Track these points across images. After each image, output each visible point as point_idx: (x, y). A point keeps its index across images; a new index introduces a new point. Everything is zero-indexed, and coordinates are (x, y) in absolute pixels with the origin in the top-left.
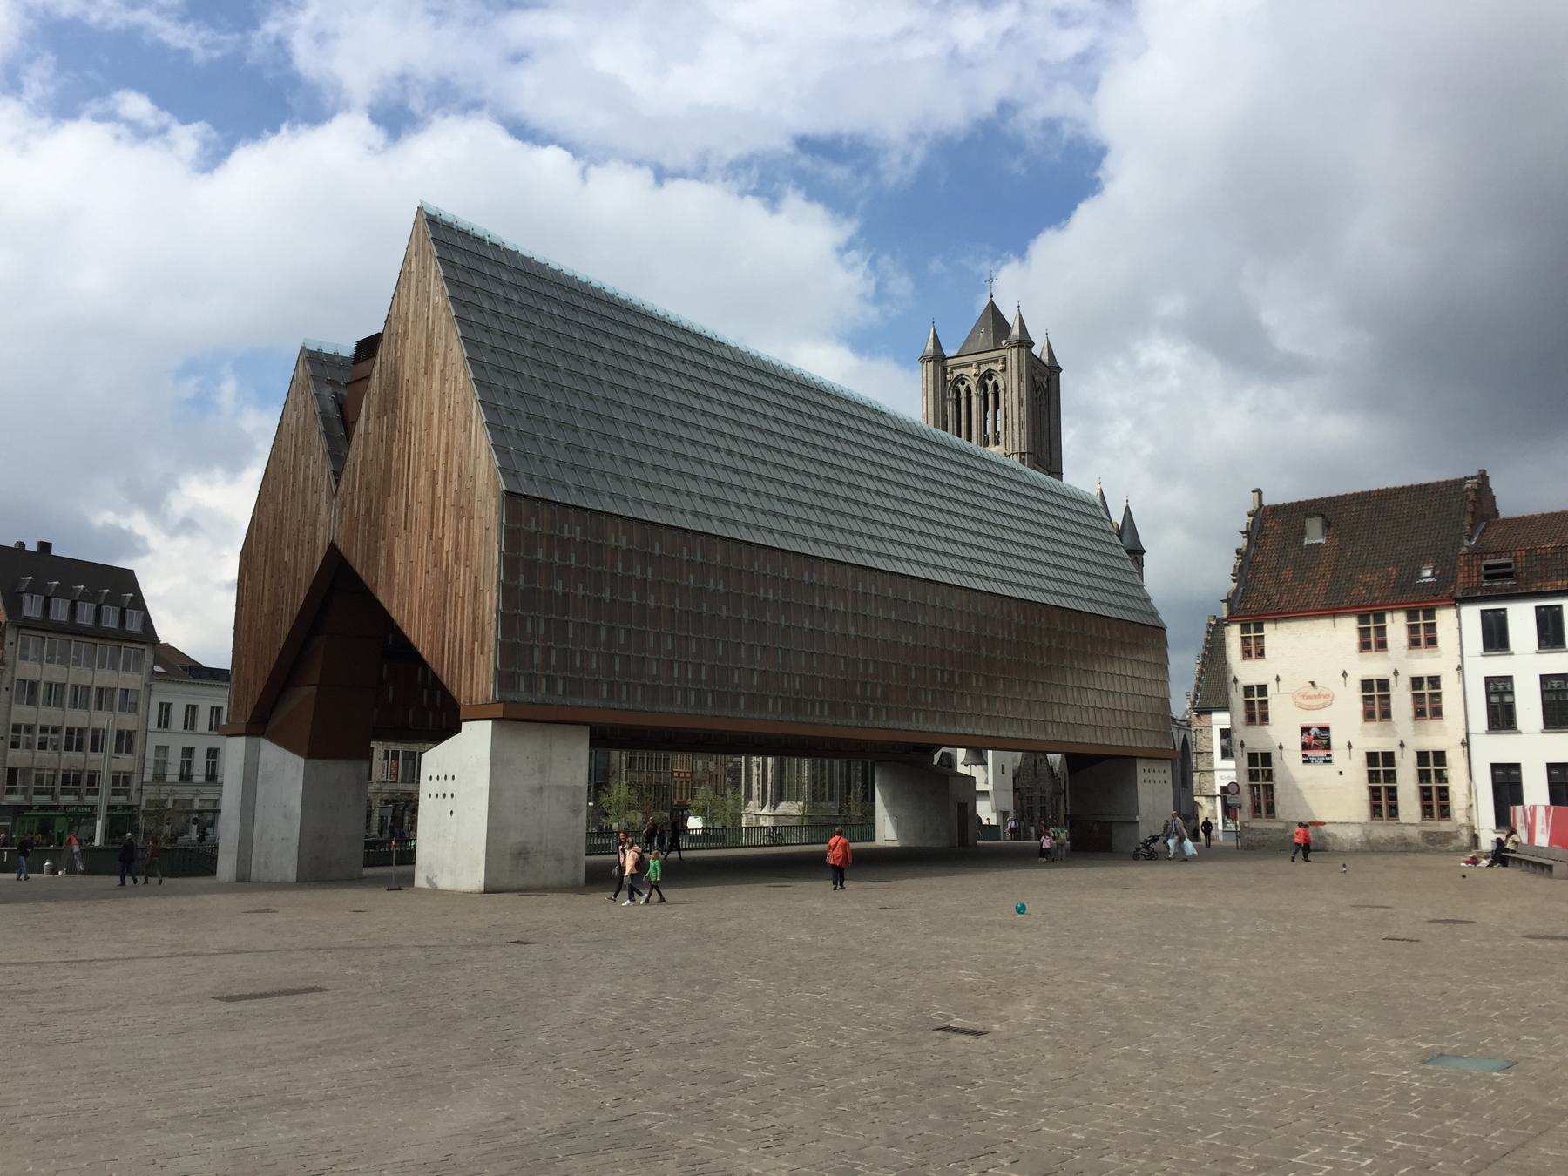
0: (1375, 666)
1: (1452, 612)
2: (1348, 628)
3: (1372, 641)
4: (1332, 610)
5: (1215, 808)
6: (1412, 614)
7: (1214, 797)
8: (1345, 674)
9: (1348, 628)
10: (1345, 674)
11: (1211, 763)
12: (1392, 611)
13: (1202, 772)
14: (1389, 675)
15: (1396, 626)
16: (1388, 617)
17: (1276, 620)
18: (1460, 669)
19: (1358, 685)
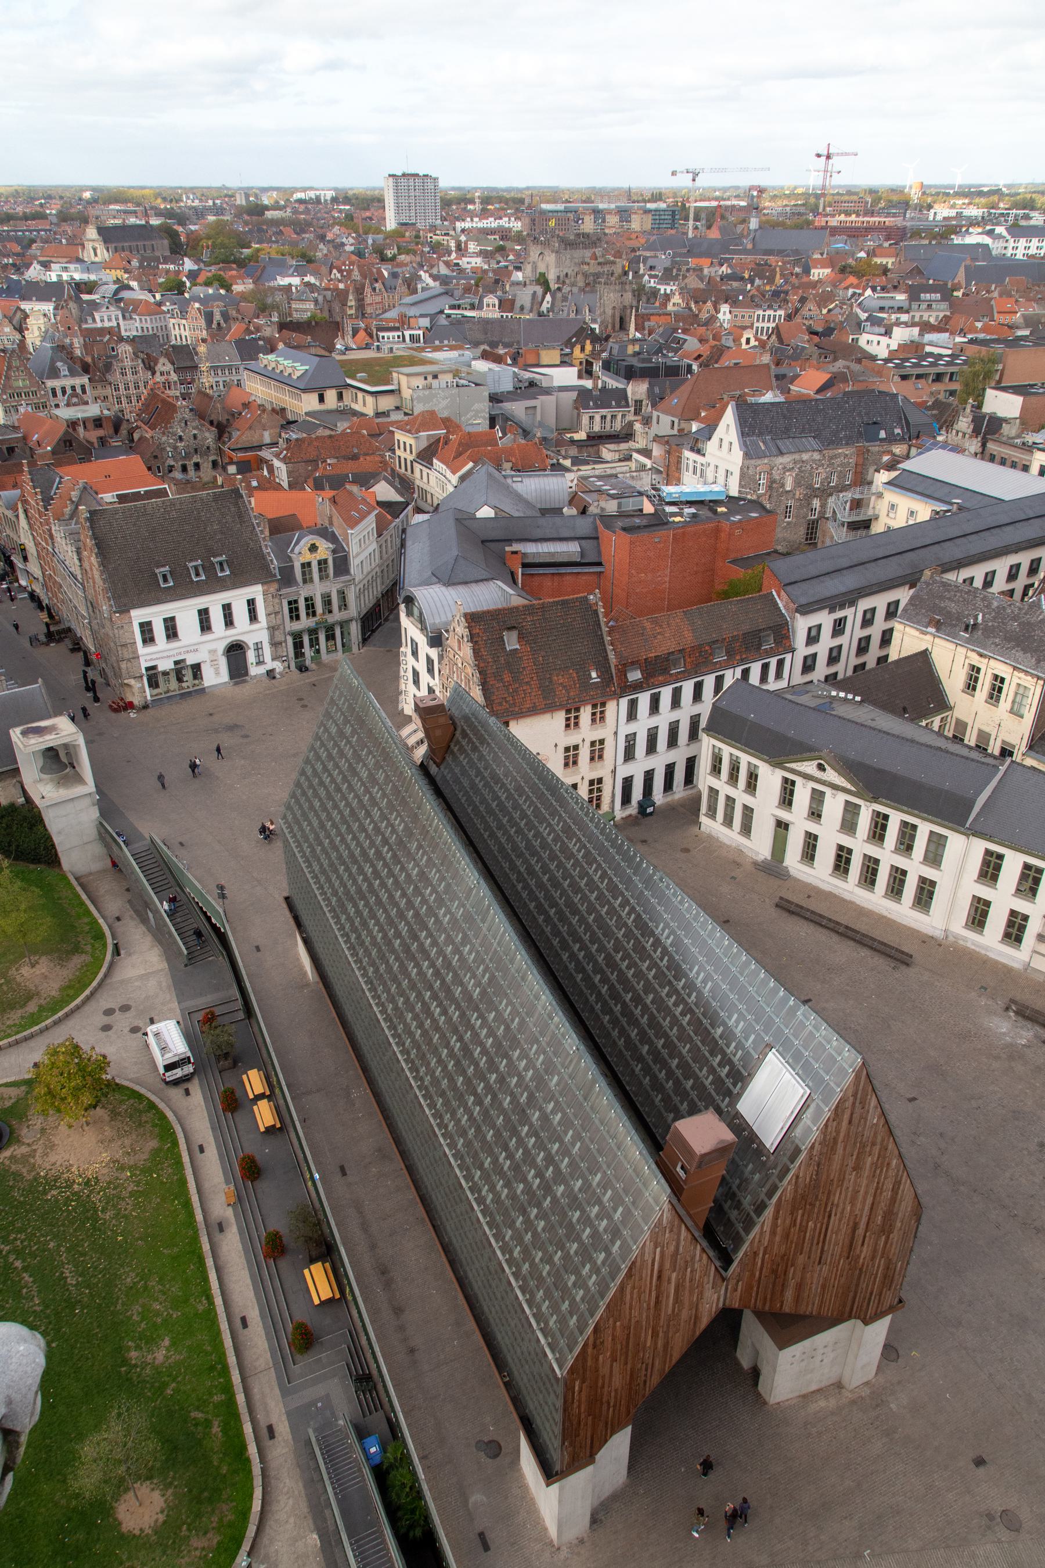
0: (573, 739)
1: (615, 702)
2: (560, 717)
3: (572, 724)
4: (550, 708)
5: (143, 684)
6: (594, 706)
7: (141, 677)
8: (556, 745)
9: (560, 717)
10: (556, 745)
11: (135, 651)
12: (584, 705)
13: (129, 660)
14: (580, 742)
15: (586, 714)
16: (582, 710)
17: (517, 719)
18: (616, 733)
19: (563, 750)
